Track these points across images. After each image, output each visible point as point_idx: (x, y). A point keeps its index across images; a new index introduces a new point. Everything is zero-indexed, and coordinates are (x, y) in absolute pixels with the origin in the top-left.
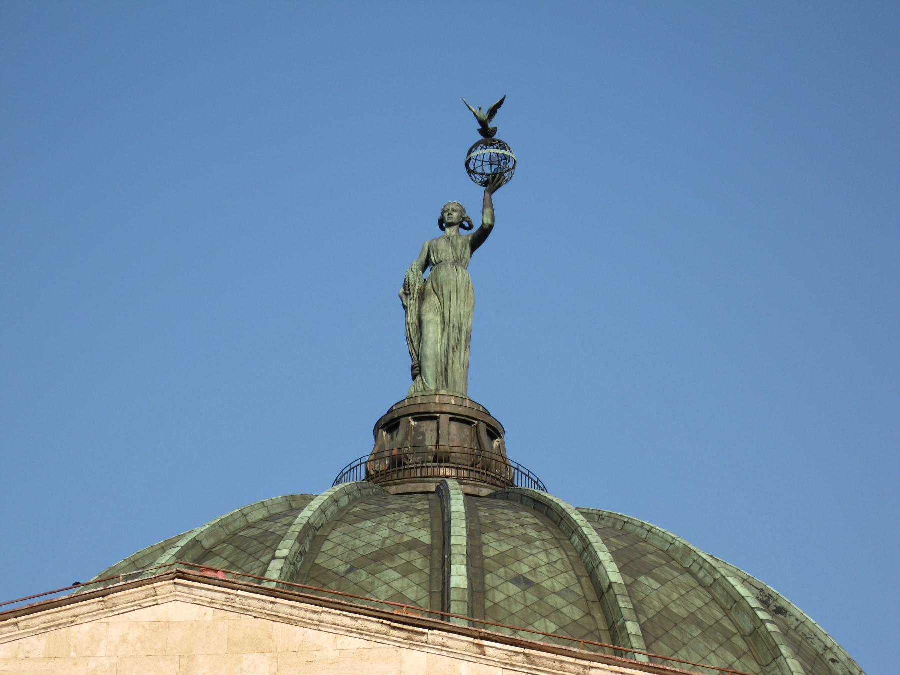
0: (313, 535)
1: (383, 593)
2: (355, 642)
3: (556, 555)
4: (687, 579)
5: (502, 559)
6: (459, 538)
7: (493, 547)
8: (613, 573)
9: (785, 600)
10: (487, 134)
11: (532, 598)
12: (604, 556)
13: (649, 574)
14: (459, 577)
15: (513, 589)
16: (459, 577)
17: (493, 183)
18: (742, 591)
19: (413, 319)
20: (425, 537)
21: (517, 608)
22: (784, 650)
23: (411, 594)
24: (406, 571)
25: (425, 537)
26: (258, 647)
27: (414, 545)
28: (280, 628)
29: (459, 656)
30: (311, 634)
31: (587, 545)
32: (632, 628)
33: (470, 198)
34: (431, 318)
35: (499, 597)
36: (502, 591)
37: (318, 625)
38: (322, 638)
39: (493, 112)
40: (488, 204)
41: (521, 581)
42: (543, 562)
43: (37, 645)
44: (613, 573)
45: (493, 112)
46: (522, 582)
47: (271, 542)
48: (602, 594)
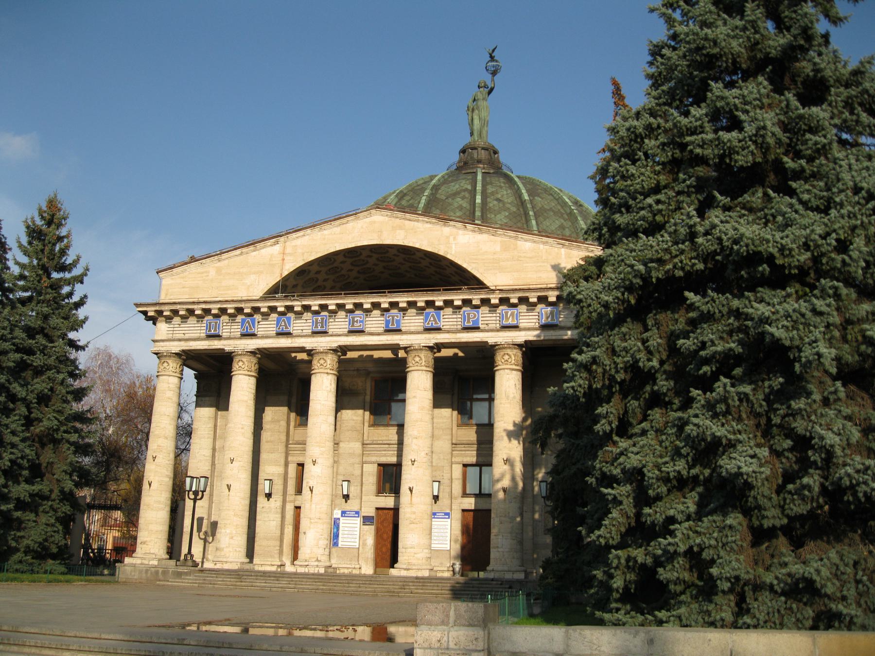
0: (436, 188)
1: (456, 205)
2: (428, 225)
3: (509, 191)
4: (551, 197)
5: (493, 193)
6: (479, 187)
7: (490, 189)
8: (526, 197)
9: (582, 202)
10: (492, 58)
11: (501, 205)
12: (524, 191)
13: (538, 196)
14: (478, 200)
15: (495, 202)
16: (478, 200)
17: (494, 73)
18: (567, 200)
19: (470, 118)
20: (469, 187)
21: (496, 208)
22: (579, 218)
23: (464, 205)
24: (463, 198)
25: (469, 187)
26: (401, 228)
27: (466, 190)
28: (407, 222)
29: (459, 229)
30: (416, 223)
31: (519, 188)
32: (531, 213)
33: (487, 78)
34: (476, 118)
35: (491, 205)
36: (492, 203)
37: (418, 221)
38: (419, 225)
39: (493, 51)
40: (493, 80)
41: (498, 200)
42: (506, 194)
43: (337, 230)
44: (526, 197)
45: (493, 51)
46: (498, 200)
47: (423, 190)
48: (523, 203)
